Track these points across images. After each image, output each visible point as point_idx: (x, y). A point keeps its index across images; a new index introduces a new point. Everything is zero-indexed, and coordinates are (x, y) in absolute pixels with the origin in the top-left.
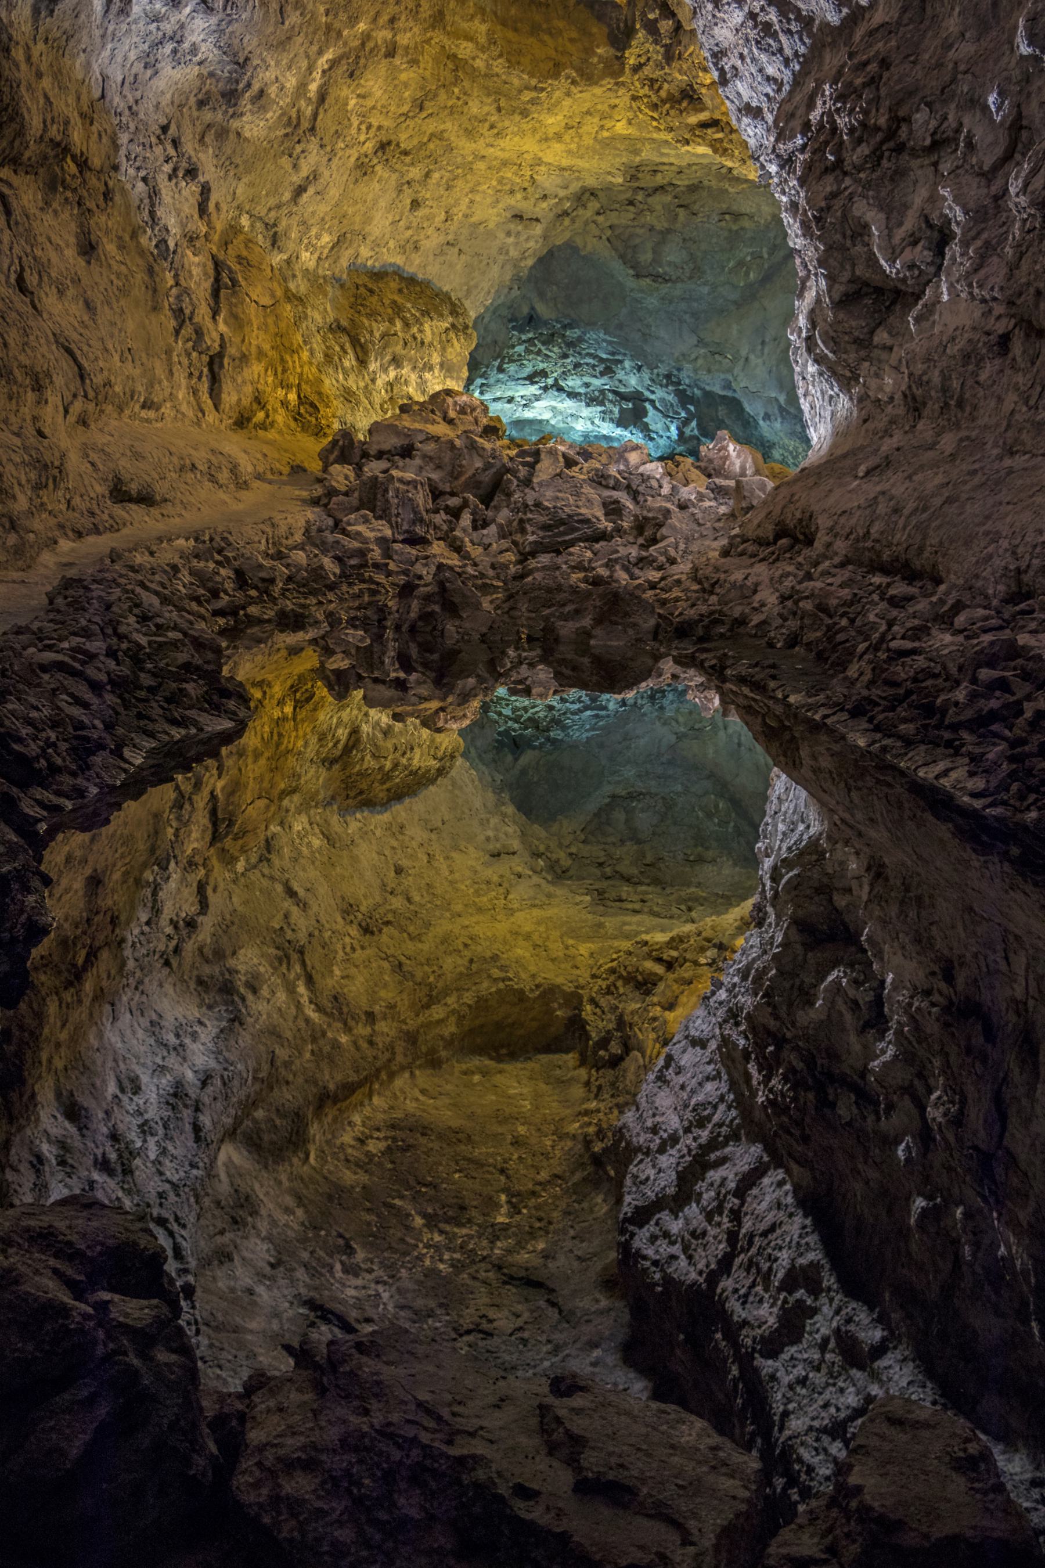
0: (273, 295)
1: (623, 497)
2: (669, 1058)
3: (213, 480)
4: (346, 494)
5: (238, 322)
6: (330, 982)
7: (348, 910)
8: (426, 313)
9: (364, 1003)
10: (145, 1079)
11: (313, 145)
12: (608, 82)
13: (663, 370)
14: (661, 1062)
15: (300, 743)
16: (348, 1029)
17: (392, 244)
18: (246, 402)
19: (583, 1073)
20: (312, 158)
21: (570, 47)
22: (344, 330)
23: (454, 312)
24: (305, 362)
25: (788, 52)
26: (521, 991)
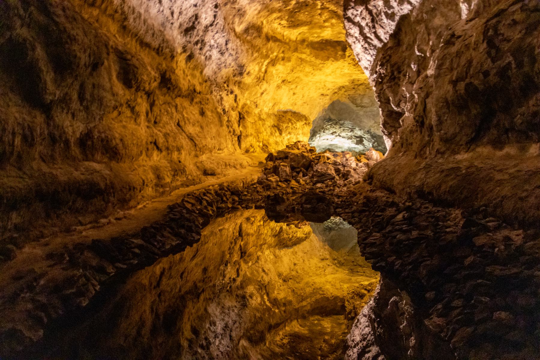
0: (255, 120)
1: (340, 167)
2: (358, 320)
3: (235, 167)
4: (270, 169)
5: (245, 127)
6: (274, 295)
7: (280, 275)
8: (298, 121)
9: (283, 300)
10: (218, 323)
11: (265, 82)
12: (342, 60)
13: (366, 130)
14: (356, 321)
15: (266, 231)
16: (278, 308)
17: (289, 104)
18: (248, 147)
19: (346, 321)
20: (265, 86)
21: (332, 53)
22: (276, 126)
23: (306, 119)
24: (265, 134)
25: (372, 54)
26: (328, 298)
